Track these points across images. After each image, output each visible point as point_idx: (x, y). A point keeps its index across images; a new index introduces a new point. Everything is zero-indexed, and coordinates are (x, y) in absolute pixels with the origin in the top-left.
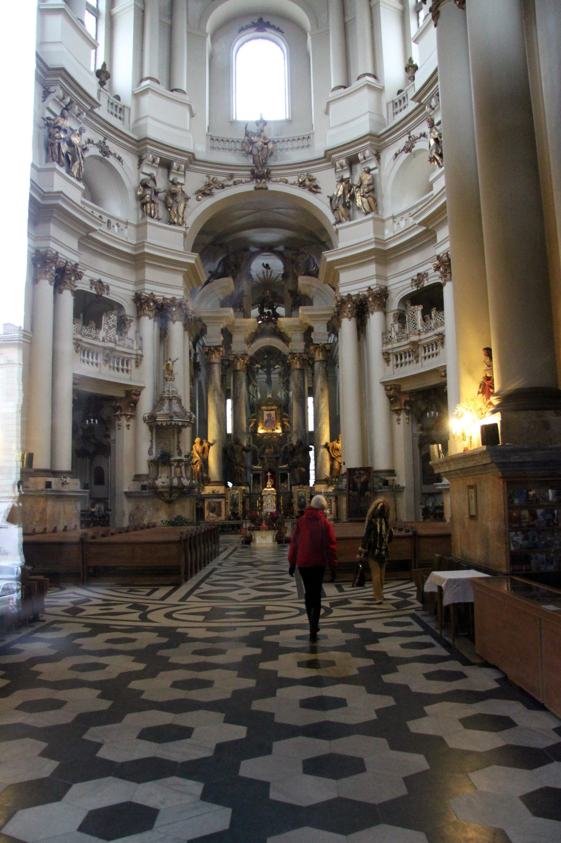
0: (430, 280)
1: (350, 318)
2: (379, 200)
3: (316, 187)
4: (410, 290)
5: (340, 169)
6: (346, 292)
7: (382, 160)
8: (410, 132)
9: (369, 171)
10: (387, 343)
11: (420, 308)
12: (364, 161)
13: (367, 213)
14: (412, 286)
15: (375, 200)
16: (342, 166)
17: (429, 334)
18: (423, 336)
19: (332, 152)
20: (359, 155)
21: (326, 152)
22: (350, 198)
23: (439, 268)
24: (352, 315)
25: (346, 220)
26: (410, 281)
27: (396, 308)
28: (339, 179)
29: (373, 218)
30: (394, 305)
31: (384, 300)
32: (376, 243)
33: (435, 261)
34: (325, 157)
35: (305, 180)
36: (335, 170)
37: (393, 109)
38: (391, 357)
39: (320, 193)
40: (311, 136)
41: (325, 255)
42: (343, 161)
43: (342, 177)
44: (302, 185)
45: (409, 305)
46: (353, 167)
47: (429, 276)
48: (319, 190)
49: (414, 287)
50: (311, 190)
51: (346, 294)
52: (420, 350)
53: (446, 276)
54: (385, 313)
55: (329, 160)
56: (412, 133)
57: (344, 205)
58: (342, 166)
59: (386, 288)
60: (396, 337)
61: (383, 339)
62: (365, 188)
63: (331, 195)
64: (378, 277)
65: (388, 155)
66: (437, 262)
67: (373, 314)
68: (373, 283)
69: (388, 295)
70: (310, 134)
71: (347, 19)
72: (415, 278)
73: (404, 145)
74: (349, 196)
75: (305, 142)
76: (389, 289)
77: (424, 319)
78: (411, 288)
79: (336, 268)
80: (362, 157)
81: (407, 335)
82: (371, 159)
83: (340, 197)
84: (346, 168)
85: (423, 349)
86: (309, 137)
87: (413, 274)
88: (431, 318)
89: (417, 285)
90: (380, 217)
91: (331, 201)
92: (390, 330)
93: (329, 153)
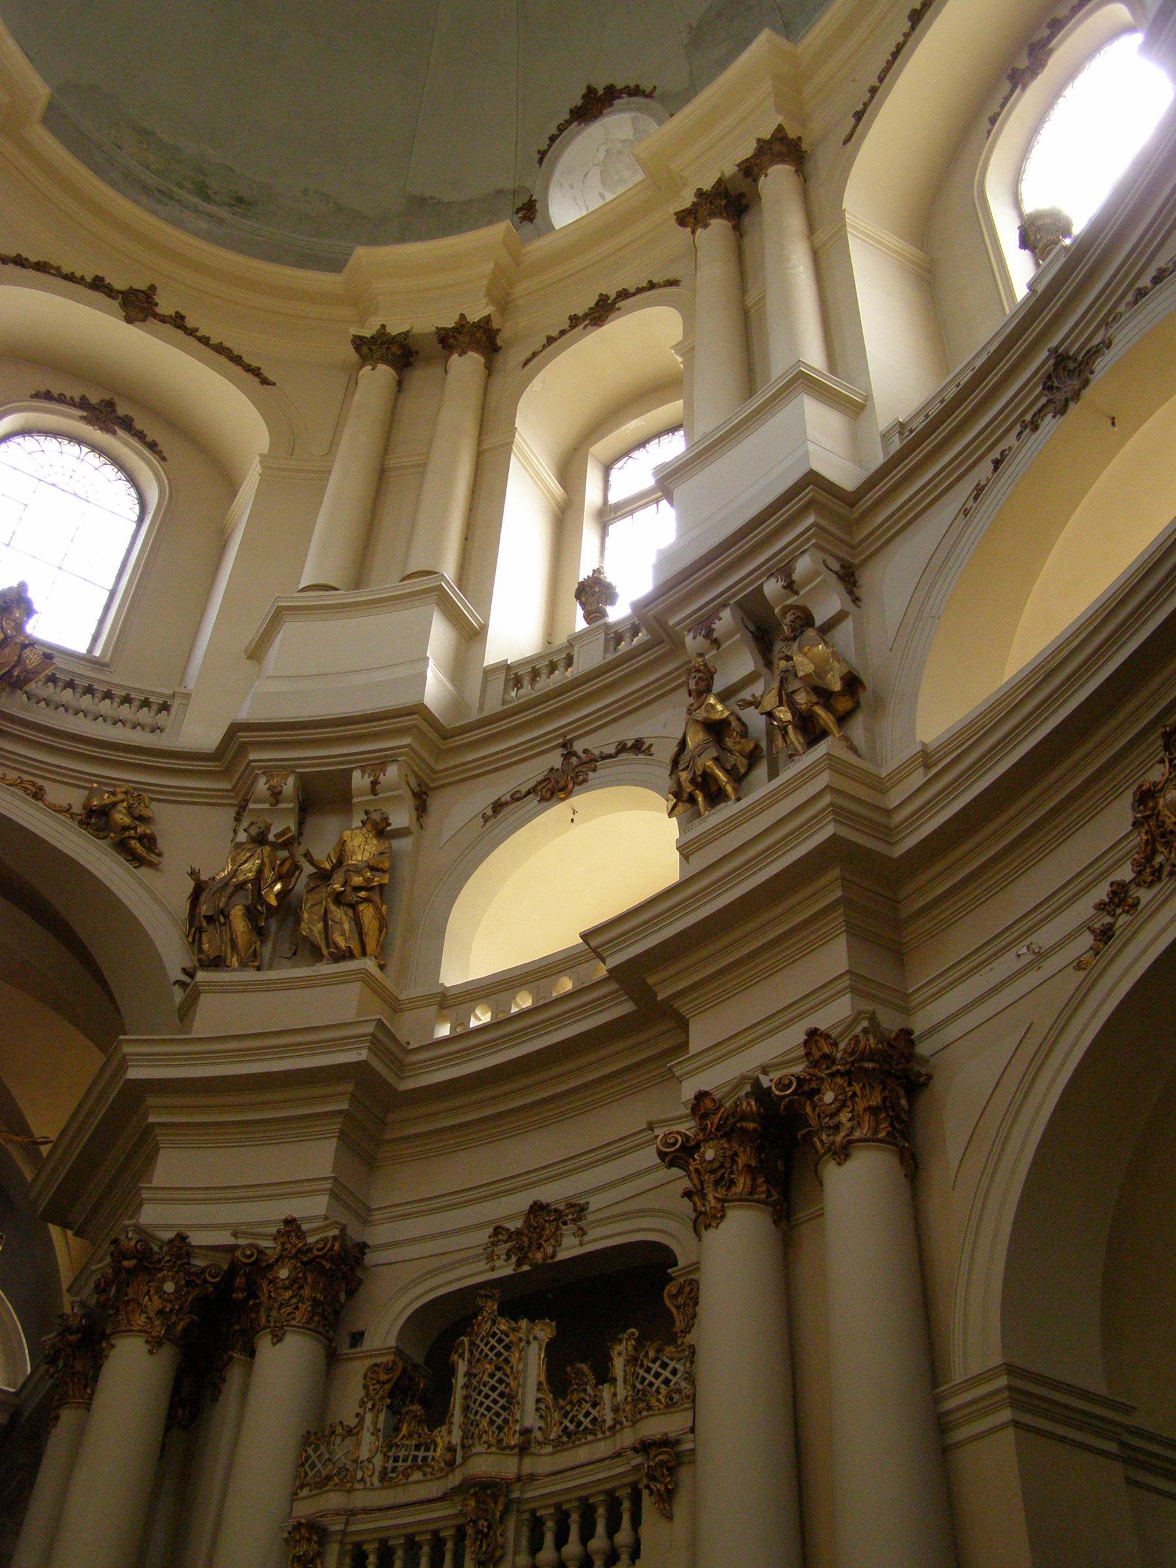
0: (592, 1234)
1: (155, 1344)
2: (398, 930)
3: (149, 841)
4: (477, 1273)
5: (267, 806)
6: (170, 1227)
7: (431, 820)
8: (571, 741)
9: (381, 830)
10: (322, 1483)
11: (544, 1331)
12: (372, 797)
13: (342, 956)
14: (490, 1257)
15: (383, 924)
16: (276, 795)
17: (582, 1454)
18: (529, 1465)
19: (256, 736)
20: (356, 776)
21: (235, 729)
22: (279, 895)
23: (697, 1147)
24: (170, 1329)
25: (244, 965)
26: (483, 1236)
27: (392, 1342)
28: (254, 831)
29: (366, 978)
30: (384, 1323)
31: (342, 1297)
32: (375, 1043)
33: (679, 1119)
34: (216, 755)
35: (114, 804)
36: (242, 808)
37: (505, 691)
38: (333, 1549)
39: (152, 865)
40: (175, 705)
41: (126, 1049)
42: (289, 785)
43: (268, 828)
44: (96, 819)
45: (492, 1306)
46: (311, 822)
47: (590, 1218)
48: (153, 858)
49: (498, 1263)
50: (122, 847)
51: (168, 1235)
52: (511, 1523)
53: (732, 1183)
54: (332, 1358)
55: (225, 773)
56: (579, 747)
57: (251, 914)
58: (276, 795)
59: (363, 1247)
60: (378, 1460)
61: (303, 1463)
62: (359, 872)
63: (204, 877)
64: (339, 1192)
65: (460, 808)
66: (688, 1127)
67: (278, 1339)
68: (312, 1208)
69: (360, 1282)
70: (173, 696)
71: (393, 462)
72: (513, 1226)
73: (539, 778)
74: (278, 887)
75: (144, 715)
76: (370, 1258)
77: (558, 1381)
78: (483, 1265)
79: (152, 1119)
80: (367, 780)
81: (451, 1449)
82: (400, 798)
83: (241, 886)
84: (291, 805)
85: (525, 1530)
86: (165, 707)
87: (511, 1208)
88: (604, 1376)
89: (521, 1253)
90: (390, 984)
91: (195, 898)
92: (352, 1422)
93: (244, 737)
